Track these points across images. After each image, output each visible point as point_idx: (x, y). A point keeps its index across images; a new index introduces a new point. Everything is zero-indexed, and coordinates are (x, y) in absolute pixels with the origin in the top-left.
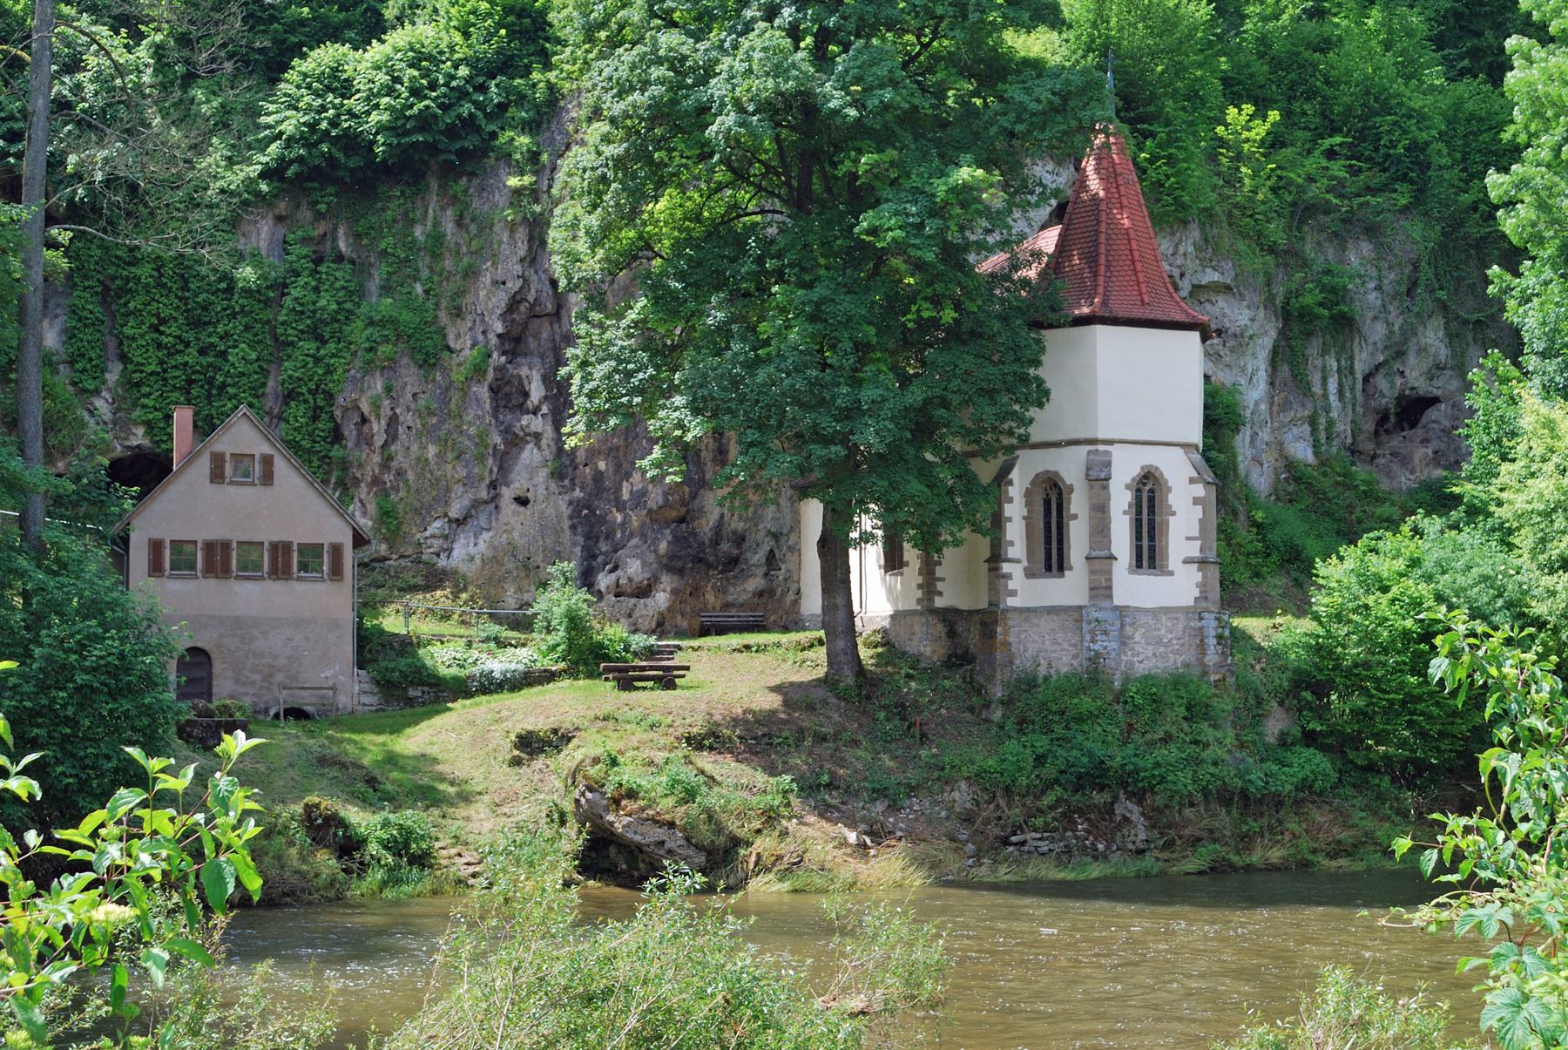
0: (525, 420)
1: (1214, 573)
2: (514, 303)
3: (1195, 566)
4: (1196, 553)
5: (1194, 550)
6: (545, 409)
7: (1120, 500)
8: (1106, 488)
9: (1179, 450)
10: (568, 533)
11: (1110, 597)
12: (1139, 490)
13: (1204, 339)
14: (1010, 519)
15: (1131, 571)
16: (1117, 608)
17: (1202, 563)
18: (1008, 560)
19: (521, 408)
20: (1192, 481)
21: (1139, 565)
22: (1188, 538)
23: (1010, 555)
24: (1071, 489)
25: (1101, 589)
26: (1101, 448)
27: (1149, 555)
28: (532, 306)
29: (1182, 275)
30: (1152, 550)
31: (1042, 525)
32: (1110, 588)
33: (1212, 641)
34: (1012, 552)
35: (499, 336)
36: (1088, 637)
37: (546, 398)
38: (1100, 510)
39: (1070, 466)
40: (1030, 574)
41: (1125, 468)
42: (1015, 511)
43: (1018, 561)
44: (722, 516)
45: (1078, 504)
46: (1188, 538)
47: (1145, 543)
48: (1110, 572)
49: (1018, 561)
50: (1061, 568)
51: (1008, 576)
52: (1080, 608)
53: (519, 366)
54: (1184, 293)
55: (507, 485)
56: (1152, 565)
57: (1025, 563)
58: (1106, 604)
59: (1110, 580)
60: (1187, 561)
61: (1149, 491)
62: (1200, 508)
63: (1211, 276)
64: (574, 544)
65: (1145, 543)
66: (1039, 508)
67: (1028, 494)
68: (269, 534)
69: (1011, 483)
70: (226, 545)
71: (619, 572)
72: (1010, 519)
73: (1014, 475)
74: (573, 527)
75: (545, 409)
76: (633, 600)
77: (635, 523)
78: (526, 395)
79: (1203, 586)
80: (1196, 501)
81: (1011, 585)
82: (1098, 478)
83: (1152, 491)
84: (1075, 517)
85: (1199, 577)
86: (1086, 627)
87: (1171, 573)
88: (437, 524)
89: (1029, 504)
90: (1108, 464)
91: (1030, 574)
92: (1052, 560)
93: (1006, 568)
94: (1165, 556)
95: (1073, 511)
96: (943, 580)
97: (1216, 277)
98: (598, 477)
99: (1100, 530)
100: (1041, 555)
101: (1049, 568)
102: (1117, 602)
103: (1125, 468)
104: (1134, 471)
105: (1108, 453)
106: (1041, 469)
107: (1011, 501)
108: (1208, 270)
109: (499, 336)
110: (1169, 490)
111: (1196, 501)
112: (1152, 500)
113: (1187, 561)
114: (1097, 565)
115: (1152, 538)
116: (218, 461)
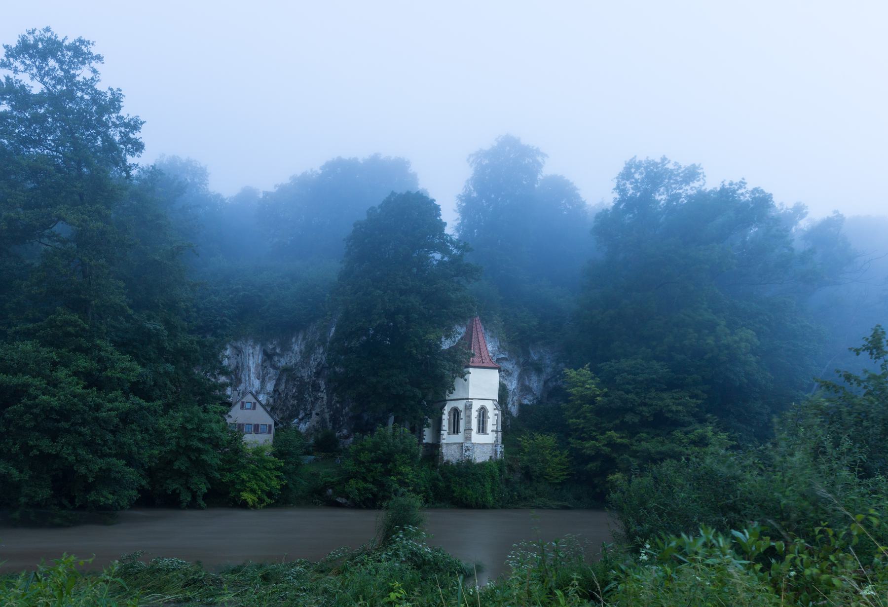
0: (319, 394)
1: (500, 434)
2: (319, 364)
3: (495, 432)
4: (495, 429)
5: (495, 428)
6: (325, 391)
7: (474, 414)
8: (471, 411)
9: (491, 401)
10: (329, 423)
11: (471, 440)
12: (480, 412)
13: (500, 372)
14: (444, 419)
15: (477, 434)
16: (472, 443)
17: (497, 431)
18: (443, 430)
19: (318, 391)
20: (495, 409)
21: (479, 432)
22: (493, 425)
23: (444, 429)
24: (461, 411)
25: (468, 438)
26: (470, 400)
27: (482, 429)
28: (323, 365)
29: (494, 356)
30: (483, 428)
31: (453, 421)
32: (471, 438)
33: (499, 453)
34: (444, 428)
35: (314, 373)
36: (464, 451)
37: (325, 388)
38: (469, 417)
39: (461, 405)
40: (449, 434)
41: (476, 405)
42: (445, 417)
43: (446, 431)
44: (368, 418)
45: (462, 415)
46: (493, 425)
47: (481, 426)
48: (471, 434)
49: (446, 431)
50: (457, 433)
51: (443, 435)
52: (462, 443)
53: (319, 380)
54: (495, 360)
55: (314, 410)
56: (483, 432)
57: (448, 431)
58: (470, 442)
59: (471, 436)
60: (493, 431)
61: (483, 412)
62: (496, 417)
63: (502, 356)
64: (330, 426)
65: (481, 426)
66: (452, 417)
67: (449, 413)
68: (254, 422)
69: (445, 410)
70: (243, 425)
71: (341, 433)
72: (444, 419)
73: (446, 408)
74: (330, 421)
75: (325, 391)
76: (344, 440)
77: (346, 420)
78: (320, 387)
79: (497, 438)
80: (496, 415)
81: (444, 437)
82: (469, 408)
83: (483, 412)
84: (462, 419)
85: (496, 435)
86: (464, 448)
87: (488, 434)
88: (296, 420)
89: (449, 415)
90: (472, 405)
91: (449, 434)
92: (455, 430)
93: (442, 432)
94: (486, 429)
95: (461, 417)
96: (425, 435)
97: (503, 356)
98: (337, 408)
99: (469, 422)
100: (452, 429)
101: (454, 433)
102: (472, 442)
103: (476, 405)
104: (479, 406)
105: (472, 402)
106: (453, 406)
107: (445, 414)
108: (501, 354)
109: (314, 373)
110: (488, 412)
111: (496, 415)
112: (483, 414)
113: (493, 431)
114: (467, 432)
115: (483, 424)
116: (243, 404)
